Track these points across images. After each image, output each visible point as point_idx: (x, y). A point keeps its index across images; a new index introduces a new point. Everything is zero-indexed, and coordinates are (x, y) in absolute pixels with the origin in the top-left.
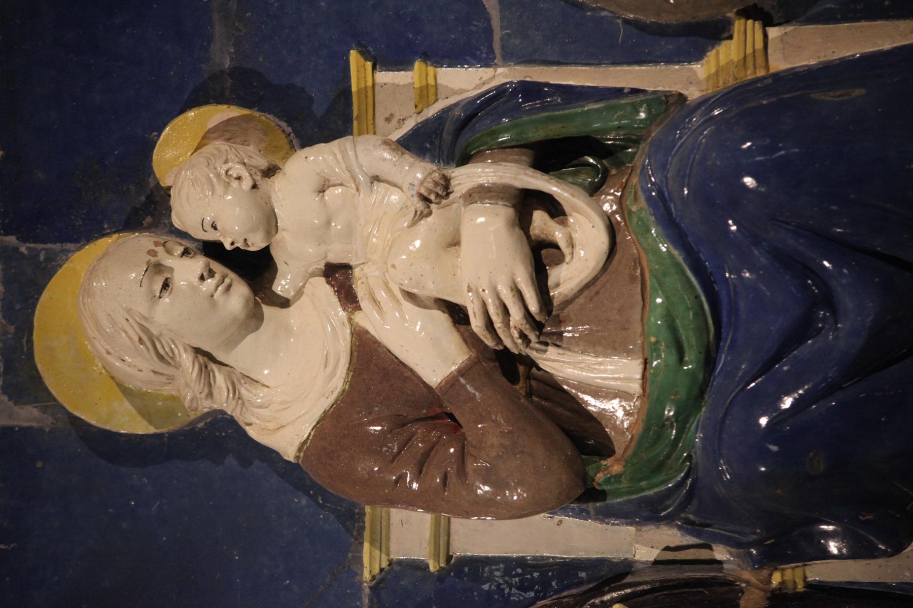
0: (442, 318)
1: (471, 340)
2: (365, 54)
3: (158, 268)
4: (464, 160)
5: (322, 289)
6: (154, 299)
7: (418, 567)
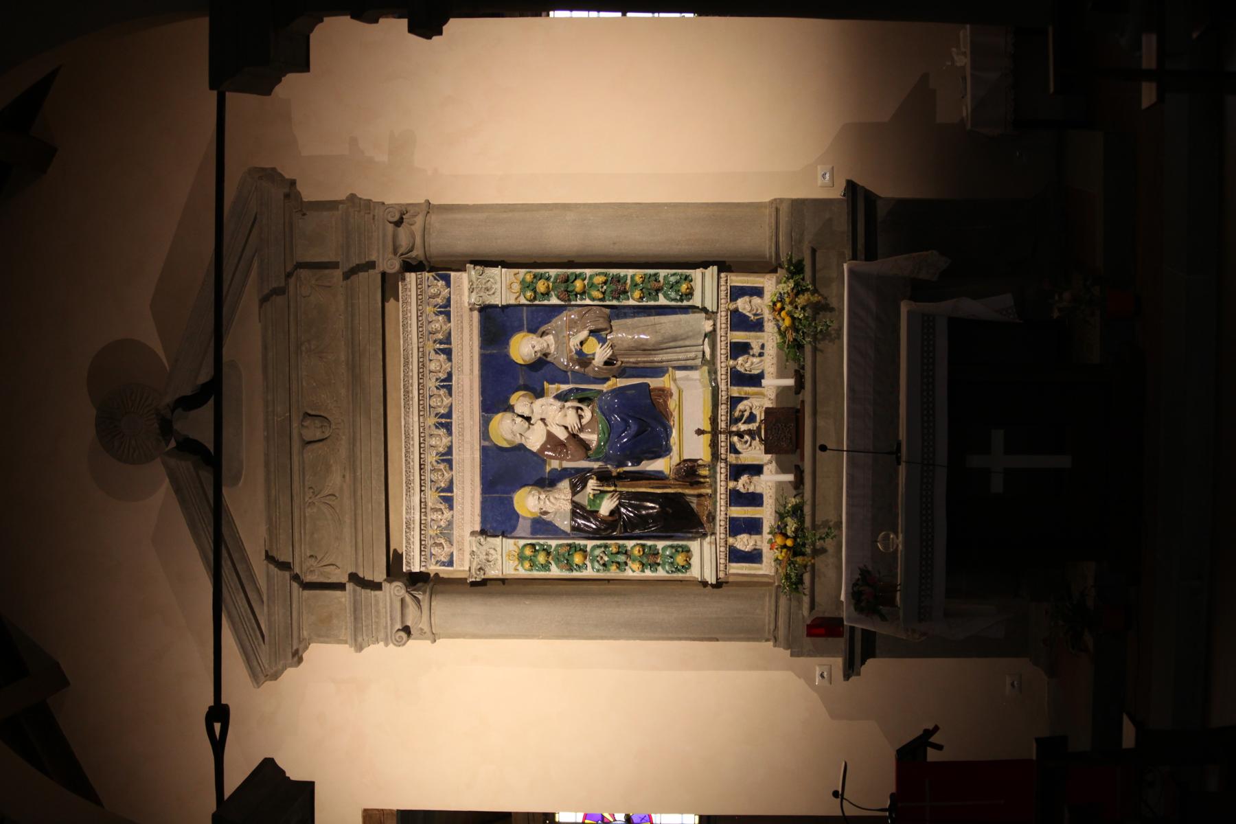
0: (563, 428)
1: (569, 432)
2: (547, 382)
3: (513, 420)
4: (566, 401)
5: (540, 422)
6: (513, 426)
7: (556, 469)
